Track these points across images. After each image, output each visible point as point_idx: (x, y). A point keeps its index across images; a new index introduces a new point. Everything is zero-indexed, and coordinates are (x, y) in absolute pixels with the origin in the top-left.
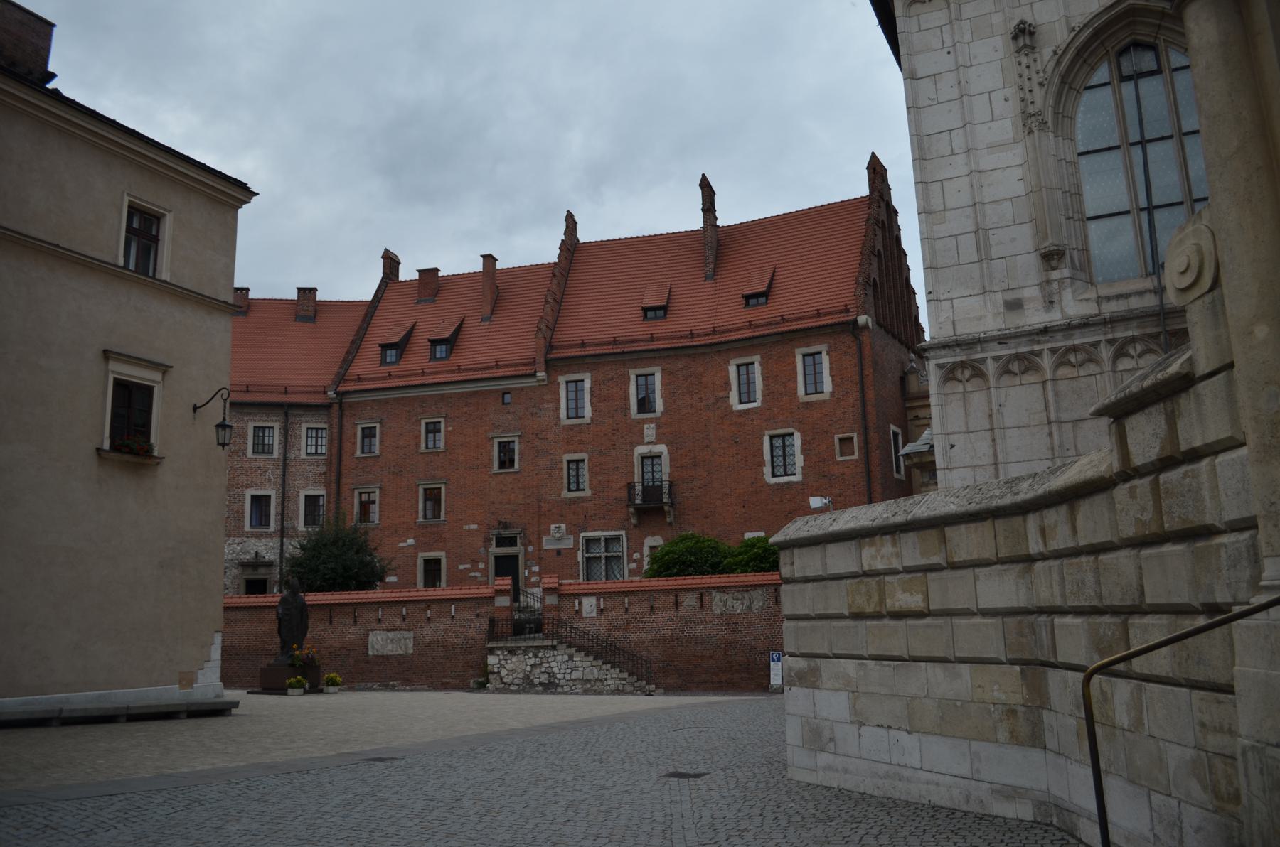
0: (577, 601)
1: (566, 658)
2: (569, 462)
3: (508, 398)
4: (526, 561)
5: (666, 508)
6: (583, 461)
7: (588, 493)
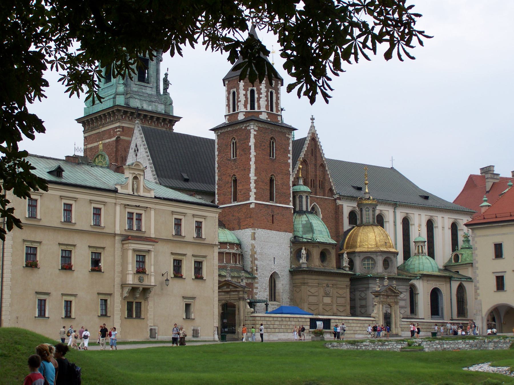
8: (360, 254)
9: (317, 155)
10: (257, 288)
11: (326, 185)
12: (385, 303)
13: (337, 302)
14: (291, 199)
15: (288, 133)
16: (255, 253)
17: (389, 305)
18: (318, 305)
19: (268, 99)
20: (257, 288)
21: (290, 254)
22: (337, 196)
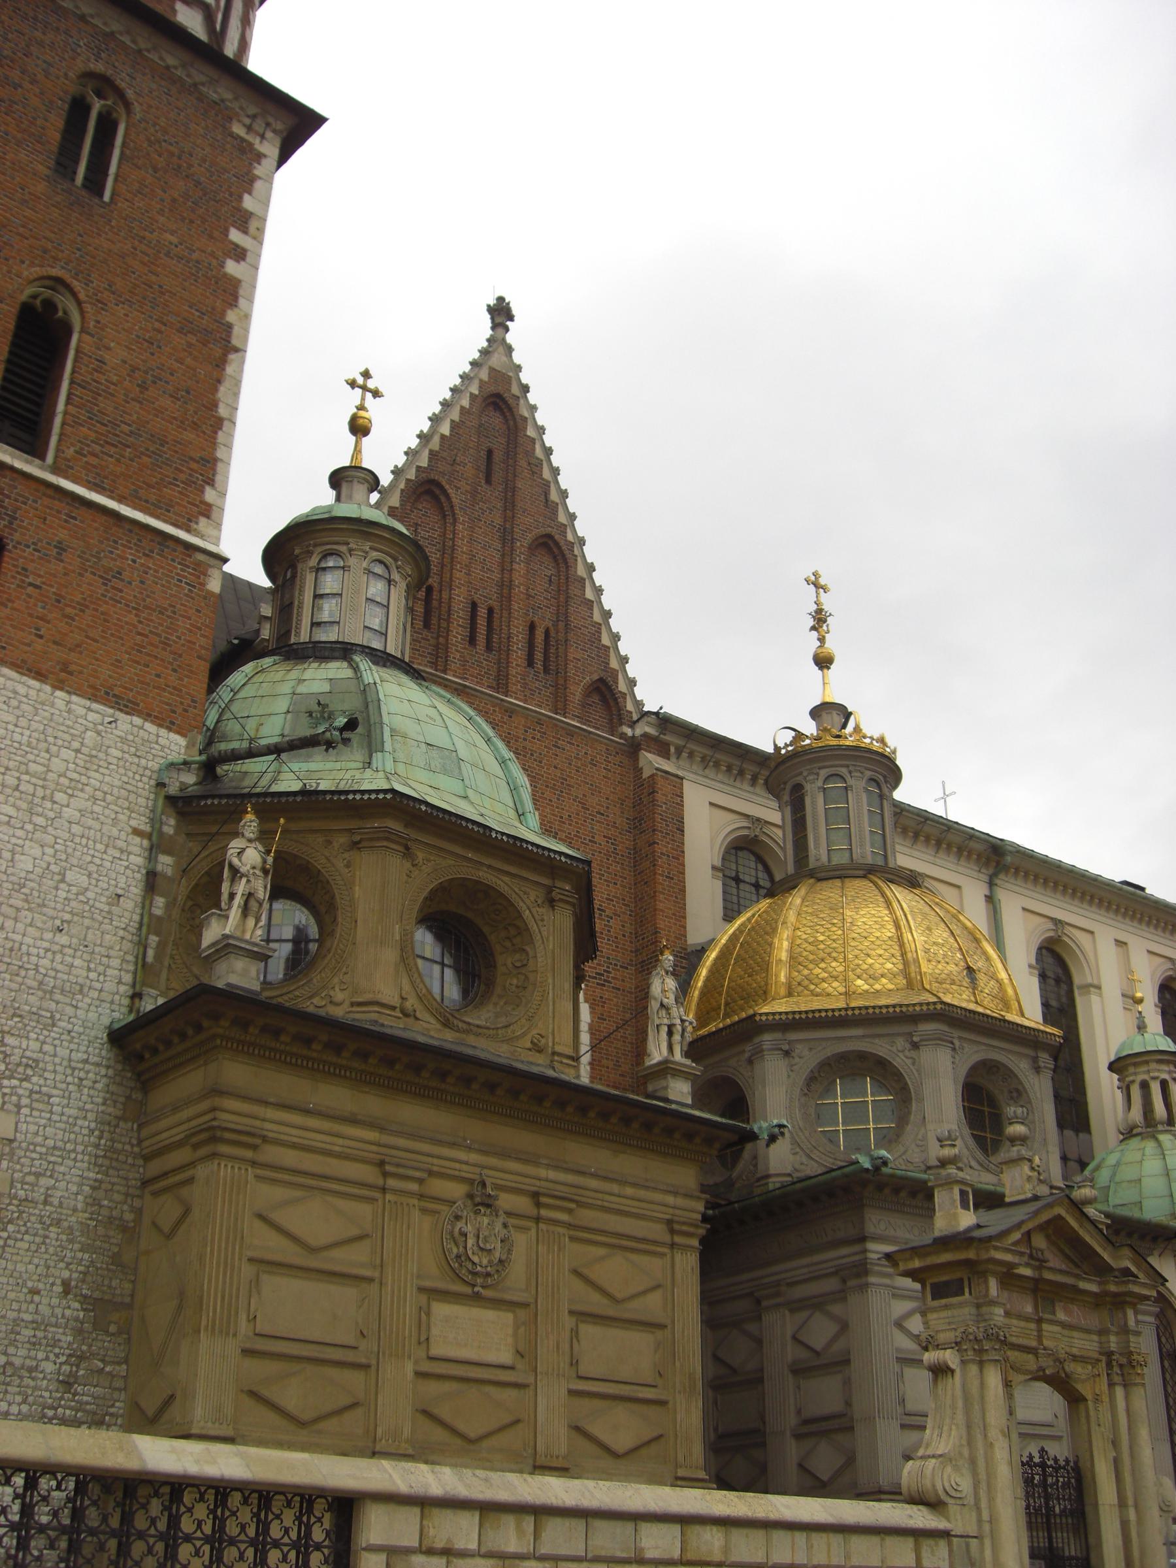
8: (793, 1036)
9: (519, 484)
12: (1030, 1362)
13: (574, 1363)
17: (1062, 1384)
21: (136, 890)
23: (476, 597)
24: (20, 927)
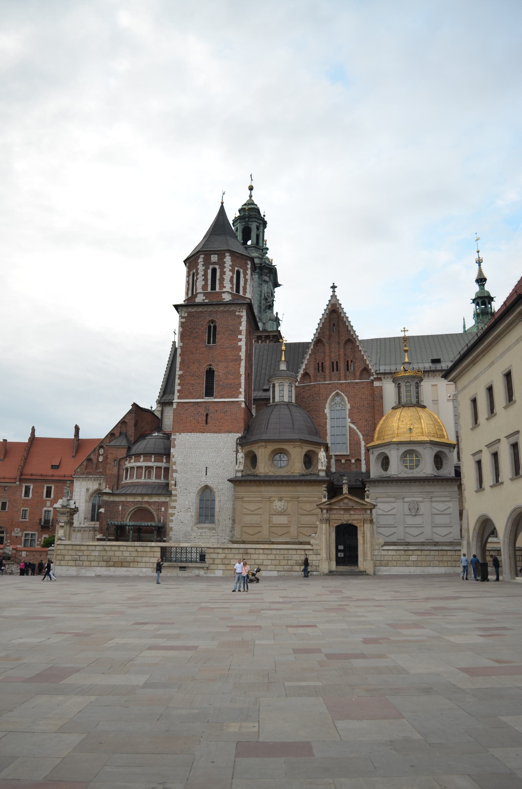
0: (21, 552)
1: (16, 567)
2: (23, 510)
3: (6, 488)
4: (6, 538)
5: (50, 527)
6: (27, 510)
7: (27, 520)
8: (374, 450)
9: (340, 330)
10: (174, 508)
11: (357, 364)
14: (242, 390)
15: (239, 311)
16: (175, 463)
18: (261, 527)
19: (207, 277)
20: (174, 508)
21: (235, 460)
22: (375, 376)
23: (333, 361)
24: (218, 471)
